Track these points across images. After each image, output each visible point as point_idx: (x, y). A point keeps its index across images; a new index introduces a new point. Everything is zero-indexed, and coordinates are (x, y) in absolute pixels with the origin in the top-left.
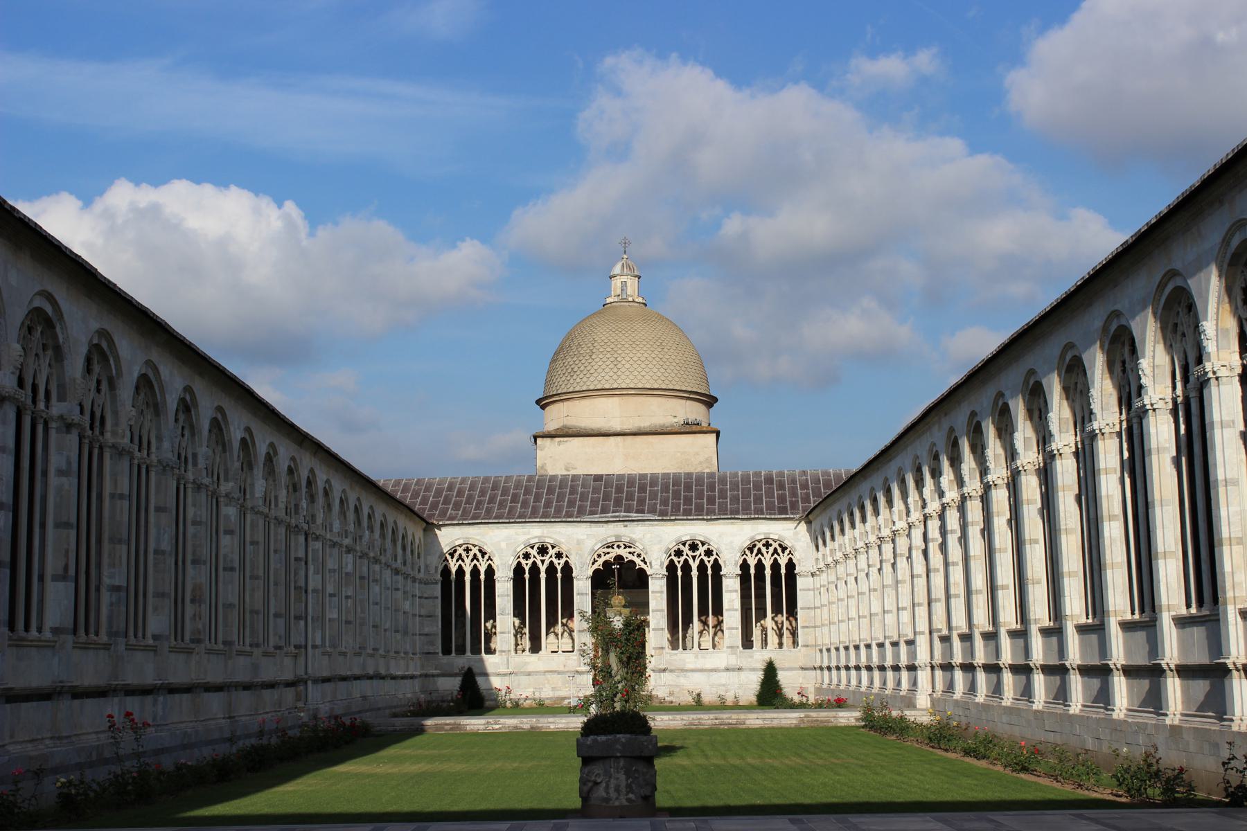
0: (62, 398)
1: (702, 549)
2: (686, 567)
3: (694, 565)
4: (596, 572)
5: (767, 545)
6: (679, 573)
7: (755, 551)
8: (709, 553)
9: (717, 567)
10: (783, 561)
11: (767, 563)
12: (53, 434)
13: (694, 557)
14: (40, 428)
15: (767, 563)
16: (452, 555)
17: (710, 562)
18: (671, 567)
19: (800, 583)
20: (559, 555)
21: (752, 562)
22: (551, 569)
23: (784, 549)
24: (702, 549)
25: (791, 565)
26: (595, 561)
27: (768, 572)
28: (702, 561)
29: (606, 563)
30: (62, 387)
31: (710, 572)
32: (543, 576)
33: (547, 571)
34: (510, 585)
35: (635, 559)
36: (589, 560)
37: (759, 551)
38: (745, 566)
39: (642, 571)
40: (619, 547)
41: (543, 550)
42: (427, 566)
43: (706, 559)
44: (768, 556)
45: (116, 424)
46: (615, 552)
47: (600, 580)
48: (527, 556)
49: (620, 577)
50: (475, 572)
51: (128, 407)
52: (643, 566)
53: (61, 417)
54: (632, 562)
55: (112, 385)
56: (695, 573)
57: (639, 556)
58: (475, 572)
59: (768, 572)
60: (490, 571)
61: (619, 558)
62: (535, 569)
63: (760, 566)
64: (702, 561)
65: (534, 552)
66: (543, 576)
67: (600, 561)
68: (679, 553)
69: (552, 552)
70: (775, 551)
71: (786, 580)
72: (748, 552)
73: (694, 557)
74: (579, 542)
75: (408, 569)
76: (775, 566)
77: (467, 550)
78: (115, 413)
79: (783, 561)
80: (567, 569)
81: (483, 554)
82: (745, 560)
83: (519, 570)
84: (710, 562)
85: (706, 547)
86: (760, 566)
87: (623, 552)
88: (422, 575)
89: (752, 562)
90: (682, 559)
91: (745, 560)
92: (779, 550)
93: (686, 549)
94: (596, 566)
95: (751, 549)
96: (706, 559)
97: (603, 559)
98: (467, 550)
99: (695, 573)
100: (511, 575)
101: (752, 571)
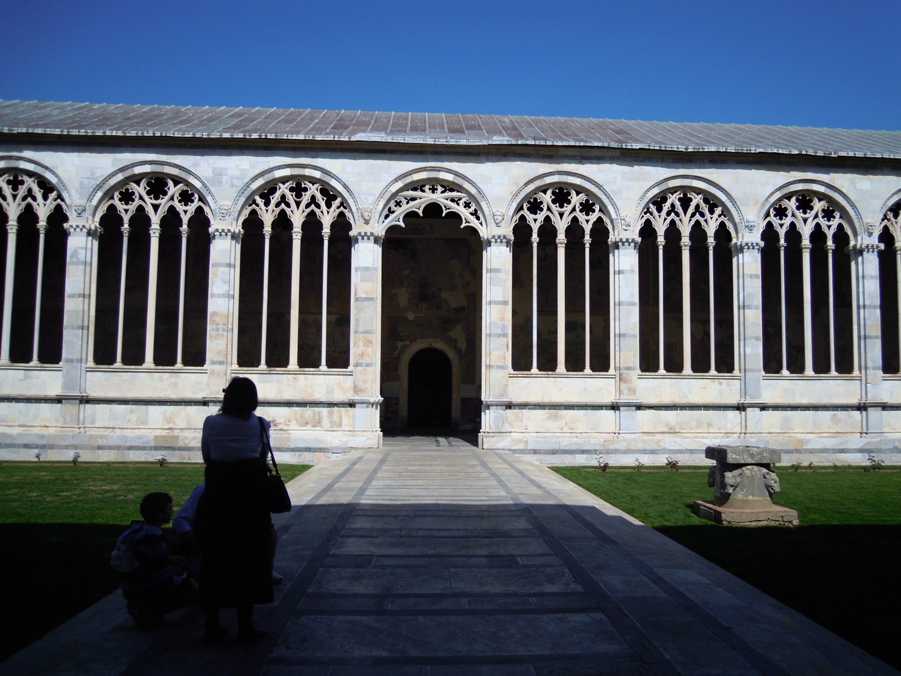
3: (561, 226)
4: (392, 230)
6: (535, 238)
7: (666, 207)
9: (600, 230)
11: (685, 229)
13: (561, 215)
15: (685, 229)
18: (522, 229)
21: (661, 227)
26: (391, 212)
27: (686, 240)
28: (575, 220)
29: (410, 216)
31: (587, 239)
35: (461, 210)
38: (647, 231)
39: (474, 231)
40: (433, 190)
43: (582, 217)
44: (685, 219)
46: (428, 197)
52: (474, 223)
54: (455, 217)
57: (467, 205)
59: (686, 240)
61: (433, 209)
63: (673, 233)
64: (575, 220)
67: (400, 212)
72: (653, 208)
73: (561, 215)
79: (711, 228)
82: (648, 222)
84: (587, 223)
85: (583, 197)
86: (673, 233)
87: (439, 197)
89: (661, 227)
90: (541, 216)
91: (648, 222)
92: (705, 209)
94: (391, 221)
96: (582, 217)
97: (405, 208)
100: (238, 228)
101: (661, 240)
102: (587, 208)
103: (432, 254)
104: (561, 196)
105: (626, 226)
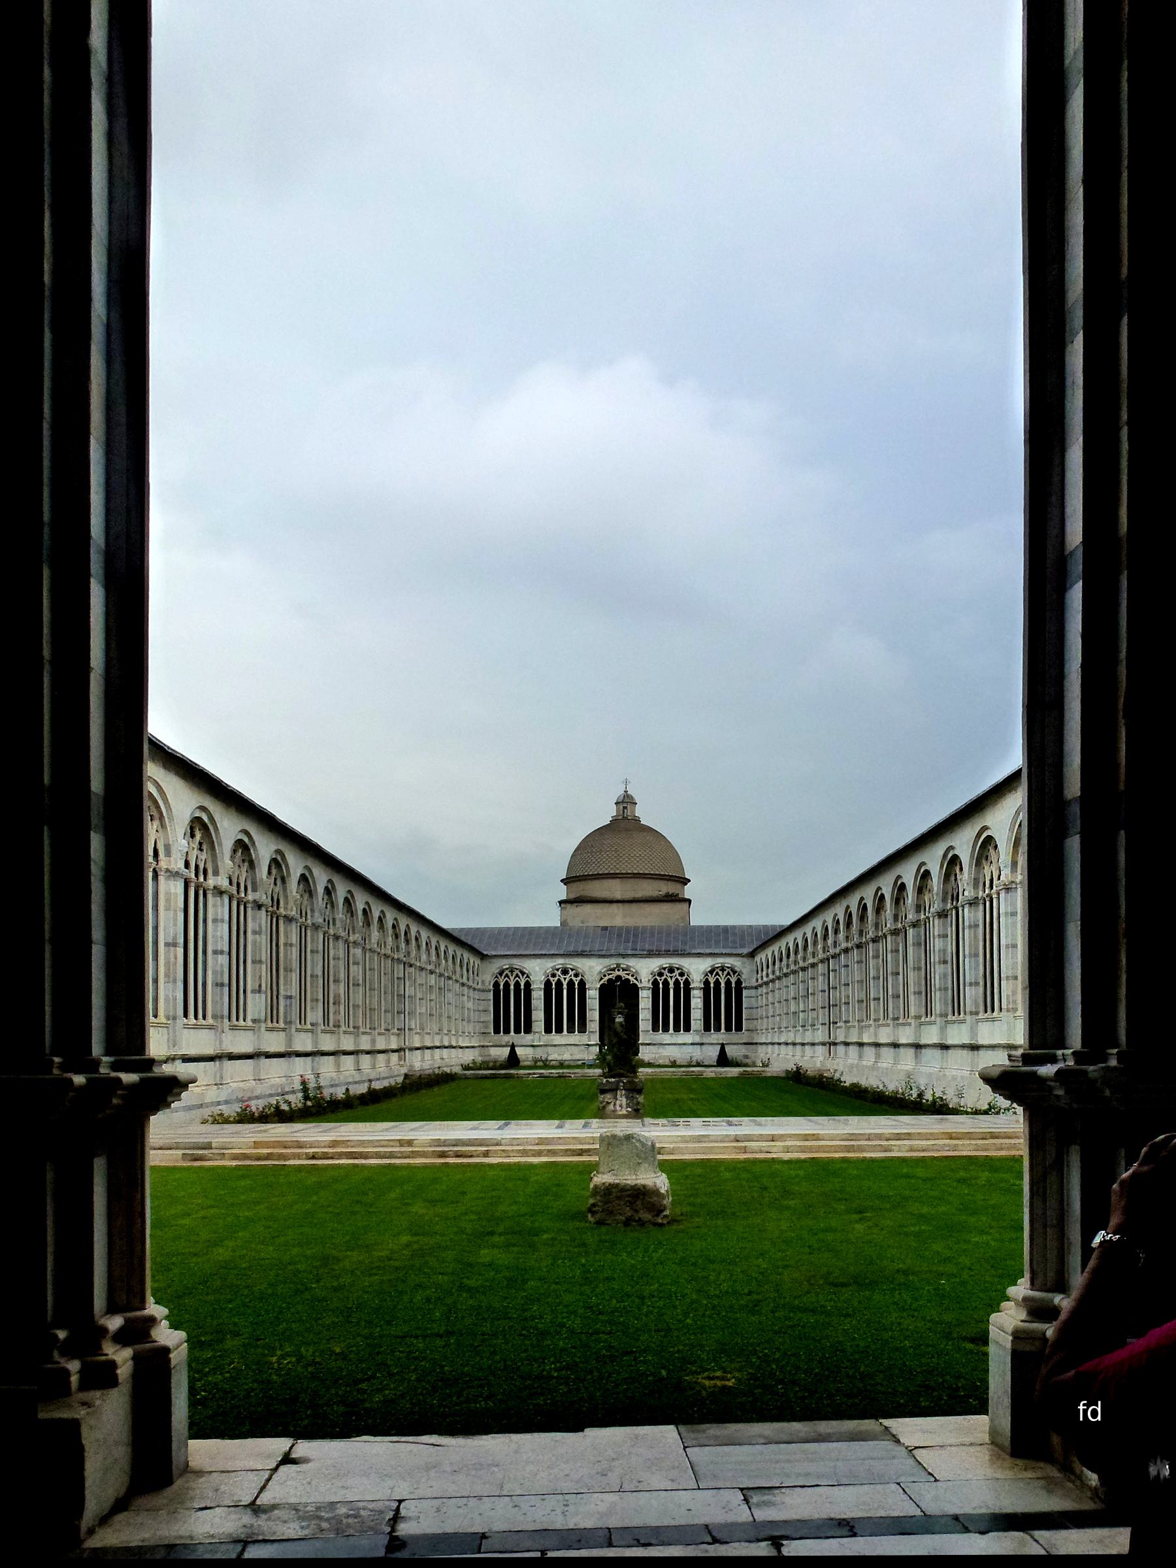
0: (254, 890)
1: (677, 972)
2: (666, 983)
5: (723, 970)
8: (682, 974)
9: (687, 983)
10: (733, 980)
12: (249, 911)
14: (242, 908)
16: (501, 974)
17: (682, 980)
19: (745, 993)
20: (576, 975)
21: (712, 980)
22: (571, 983)
23: (734, 972)
24: (677, 972)
25: (739, 982)
27: (723, 985)
29: (609, 980)
30: (254, 884)
32: (565, 986)
33: (568, 984)
34: (542, 993)
36: (598, 978)
37: (717, 974)
38: (707, 983)
41: (565, 972)
42: (483, 982)
45: (286, 903)
47: (603, 990)
48: (554, 975)
49: (620, 994)
50: (517, 984)
51: (294, 893)
53: (255, 901)
54: (628, 980)
55: (283, 880)
56: (672, 985)
58: (517, 984)
59: (723, 985)
60: (528, 984)
61: (619, 977)
62: (559, 984)
63: (717, 983)
65: (559, 973)
66: (565, 986)
68: (660, 974)
69: (571, 973)
70: (728, 974)
71: (736, 990)
74: (590, 968)
75: (470, 983)
76: (728, 983)
77: (512, 972)
78: (286, 897)
79: (733, 980)
80: (582, 984)
81: (523, 973)
83: (548, 984)
84: (682, 980)
86: (717, 983)
87: (621, 973)
88: (480, 986)
89: (712, 980)
93: (666, 972)
95: (711, 972)
98: (512, 972)
99: (672, 985)
102: (682, 974)
103: (620, 994)
104: (671, 970)
105: (697, 980)
